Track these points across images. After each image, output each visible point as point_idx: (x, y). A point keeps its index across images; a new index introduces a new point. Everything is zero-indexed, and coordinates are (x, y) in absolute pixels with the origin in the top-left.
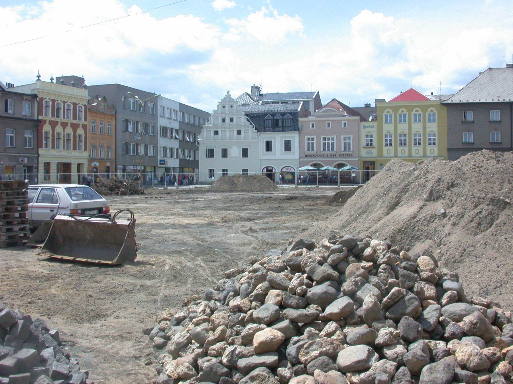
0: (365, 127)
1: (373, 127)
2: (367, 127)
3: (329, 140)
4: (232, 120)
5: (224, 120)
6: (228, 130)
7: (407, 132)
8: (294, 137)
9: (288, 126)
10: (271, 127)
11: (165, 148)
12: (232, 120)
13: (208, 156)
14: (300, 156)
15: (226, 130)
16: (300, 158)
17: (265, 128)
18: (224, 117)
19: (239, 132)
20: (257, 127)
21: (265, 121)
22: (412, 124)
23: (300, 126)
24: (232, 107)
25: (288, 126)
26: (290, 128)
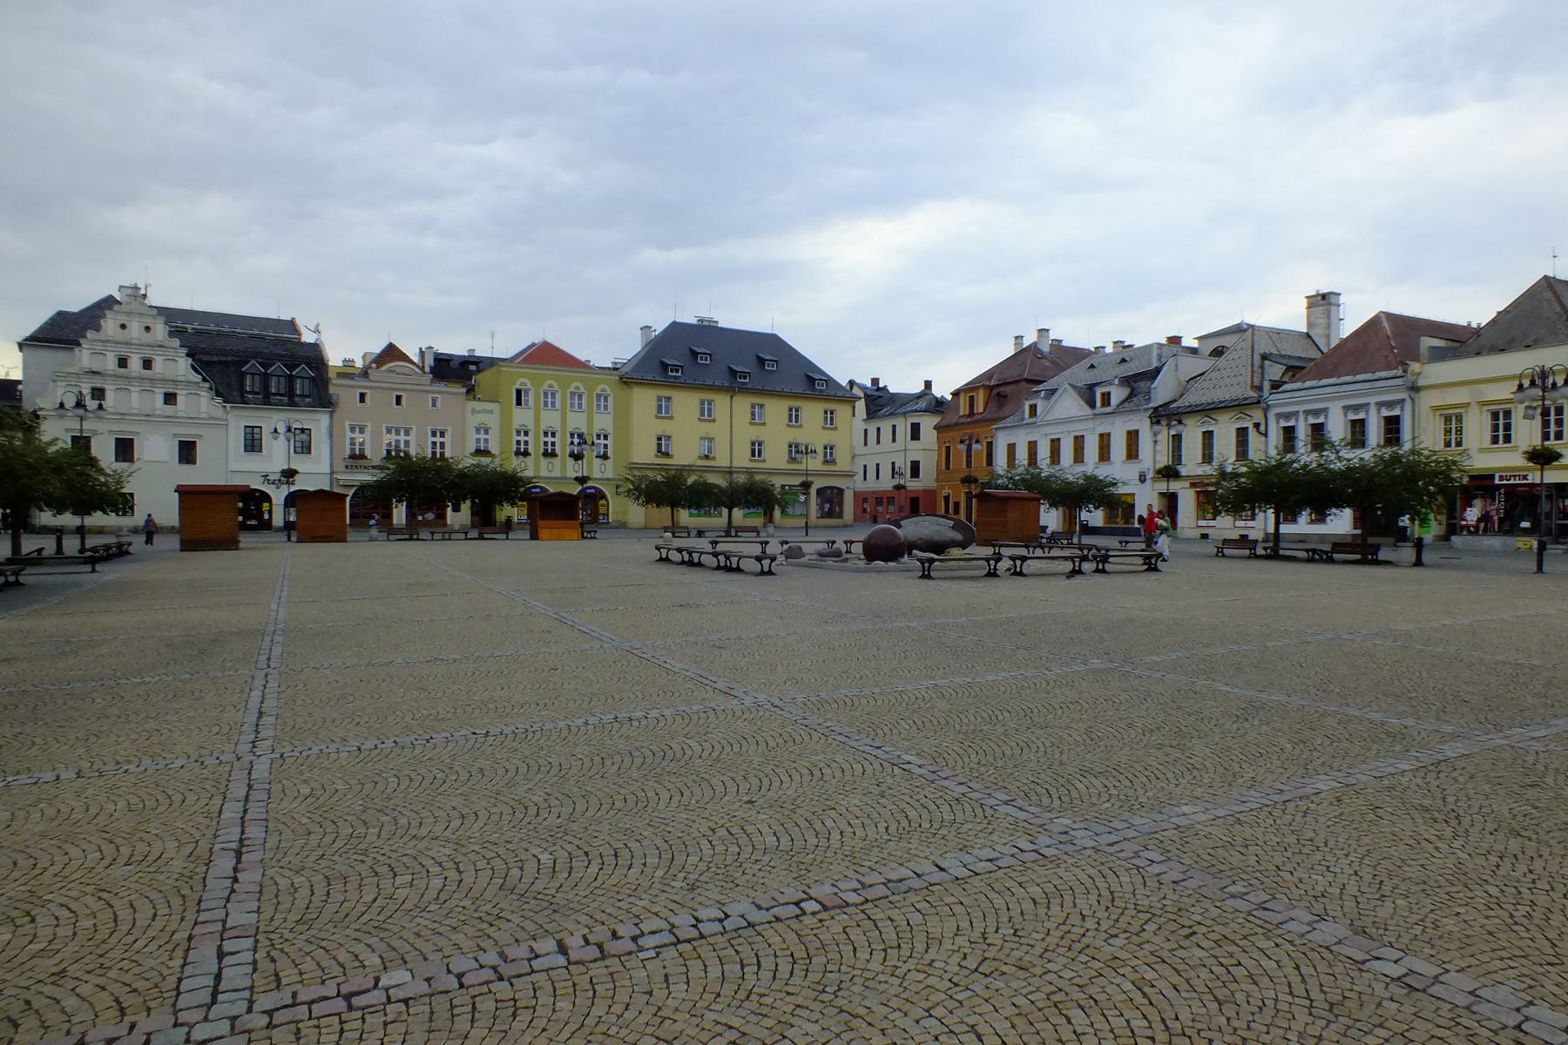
0: (474, 411)
1: (491, 412)
2: (479, 412)
3: (398, 433)
4: (147, 364)
5: (123, 362)
6: (138, 389)
7: (531, 426)
8: (318, 423)
9: (303, 396)
10: (258, 393)
11: (1325, 411)
12: (147, 364)
13: (299, 450)
14: (331, 466)
15: (156, 390)
16: (332, 473)
17: (242, 396)
18: (123, 351)
19: (170, 398)
20: (220, 389)
21: (242, 376)
22: (568, 413)
23: (334, 399)
24: (148, 329)
25: (303, 396)
26: (307, 400)
